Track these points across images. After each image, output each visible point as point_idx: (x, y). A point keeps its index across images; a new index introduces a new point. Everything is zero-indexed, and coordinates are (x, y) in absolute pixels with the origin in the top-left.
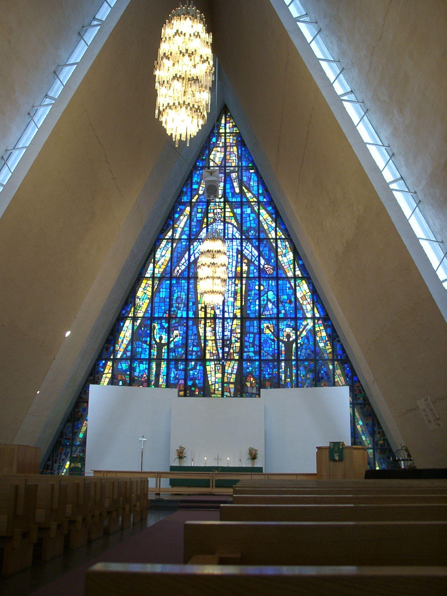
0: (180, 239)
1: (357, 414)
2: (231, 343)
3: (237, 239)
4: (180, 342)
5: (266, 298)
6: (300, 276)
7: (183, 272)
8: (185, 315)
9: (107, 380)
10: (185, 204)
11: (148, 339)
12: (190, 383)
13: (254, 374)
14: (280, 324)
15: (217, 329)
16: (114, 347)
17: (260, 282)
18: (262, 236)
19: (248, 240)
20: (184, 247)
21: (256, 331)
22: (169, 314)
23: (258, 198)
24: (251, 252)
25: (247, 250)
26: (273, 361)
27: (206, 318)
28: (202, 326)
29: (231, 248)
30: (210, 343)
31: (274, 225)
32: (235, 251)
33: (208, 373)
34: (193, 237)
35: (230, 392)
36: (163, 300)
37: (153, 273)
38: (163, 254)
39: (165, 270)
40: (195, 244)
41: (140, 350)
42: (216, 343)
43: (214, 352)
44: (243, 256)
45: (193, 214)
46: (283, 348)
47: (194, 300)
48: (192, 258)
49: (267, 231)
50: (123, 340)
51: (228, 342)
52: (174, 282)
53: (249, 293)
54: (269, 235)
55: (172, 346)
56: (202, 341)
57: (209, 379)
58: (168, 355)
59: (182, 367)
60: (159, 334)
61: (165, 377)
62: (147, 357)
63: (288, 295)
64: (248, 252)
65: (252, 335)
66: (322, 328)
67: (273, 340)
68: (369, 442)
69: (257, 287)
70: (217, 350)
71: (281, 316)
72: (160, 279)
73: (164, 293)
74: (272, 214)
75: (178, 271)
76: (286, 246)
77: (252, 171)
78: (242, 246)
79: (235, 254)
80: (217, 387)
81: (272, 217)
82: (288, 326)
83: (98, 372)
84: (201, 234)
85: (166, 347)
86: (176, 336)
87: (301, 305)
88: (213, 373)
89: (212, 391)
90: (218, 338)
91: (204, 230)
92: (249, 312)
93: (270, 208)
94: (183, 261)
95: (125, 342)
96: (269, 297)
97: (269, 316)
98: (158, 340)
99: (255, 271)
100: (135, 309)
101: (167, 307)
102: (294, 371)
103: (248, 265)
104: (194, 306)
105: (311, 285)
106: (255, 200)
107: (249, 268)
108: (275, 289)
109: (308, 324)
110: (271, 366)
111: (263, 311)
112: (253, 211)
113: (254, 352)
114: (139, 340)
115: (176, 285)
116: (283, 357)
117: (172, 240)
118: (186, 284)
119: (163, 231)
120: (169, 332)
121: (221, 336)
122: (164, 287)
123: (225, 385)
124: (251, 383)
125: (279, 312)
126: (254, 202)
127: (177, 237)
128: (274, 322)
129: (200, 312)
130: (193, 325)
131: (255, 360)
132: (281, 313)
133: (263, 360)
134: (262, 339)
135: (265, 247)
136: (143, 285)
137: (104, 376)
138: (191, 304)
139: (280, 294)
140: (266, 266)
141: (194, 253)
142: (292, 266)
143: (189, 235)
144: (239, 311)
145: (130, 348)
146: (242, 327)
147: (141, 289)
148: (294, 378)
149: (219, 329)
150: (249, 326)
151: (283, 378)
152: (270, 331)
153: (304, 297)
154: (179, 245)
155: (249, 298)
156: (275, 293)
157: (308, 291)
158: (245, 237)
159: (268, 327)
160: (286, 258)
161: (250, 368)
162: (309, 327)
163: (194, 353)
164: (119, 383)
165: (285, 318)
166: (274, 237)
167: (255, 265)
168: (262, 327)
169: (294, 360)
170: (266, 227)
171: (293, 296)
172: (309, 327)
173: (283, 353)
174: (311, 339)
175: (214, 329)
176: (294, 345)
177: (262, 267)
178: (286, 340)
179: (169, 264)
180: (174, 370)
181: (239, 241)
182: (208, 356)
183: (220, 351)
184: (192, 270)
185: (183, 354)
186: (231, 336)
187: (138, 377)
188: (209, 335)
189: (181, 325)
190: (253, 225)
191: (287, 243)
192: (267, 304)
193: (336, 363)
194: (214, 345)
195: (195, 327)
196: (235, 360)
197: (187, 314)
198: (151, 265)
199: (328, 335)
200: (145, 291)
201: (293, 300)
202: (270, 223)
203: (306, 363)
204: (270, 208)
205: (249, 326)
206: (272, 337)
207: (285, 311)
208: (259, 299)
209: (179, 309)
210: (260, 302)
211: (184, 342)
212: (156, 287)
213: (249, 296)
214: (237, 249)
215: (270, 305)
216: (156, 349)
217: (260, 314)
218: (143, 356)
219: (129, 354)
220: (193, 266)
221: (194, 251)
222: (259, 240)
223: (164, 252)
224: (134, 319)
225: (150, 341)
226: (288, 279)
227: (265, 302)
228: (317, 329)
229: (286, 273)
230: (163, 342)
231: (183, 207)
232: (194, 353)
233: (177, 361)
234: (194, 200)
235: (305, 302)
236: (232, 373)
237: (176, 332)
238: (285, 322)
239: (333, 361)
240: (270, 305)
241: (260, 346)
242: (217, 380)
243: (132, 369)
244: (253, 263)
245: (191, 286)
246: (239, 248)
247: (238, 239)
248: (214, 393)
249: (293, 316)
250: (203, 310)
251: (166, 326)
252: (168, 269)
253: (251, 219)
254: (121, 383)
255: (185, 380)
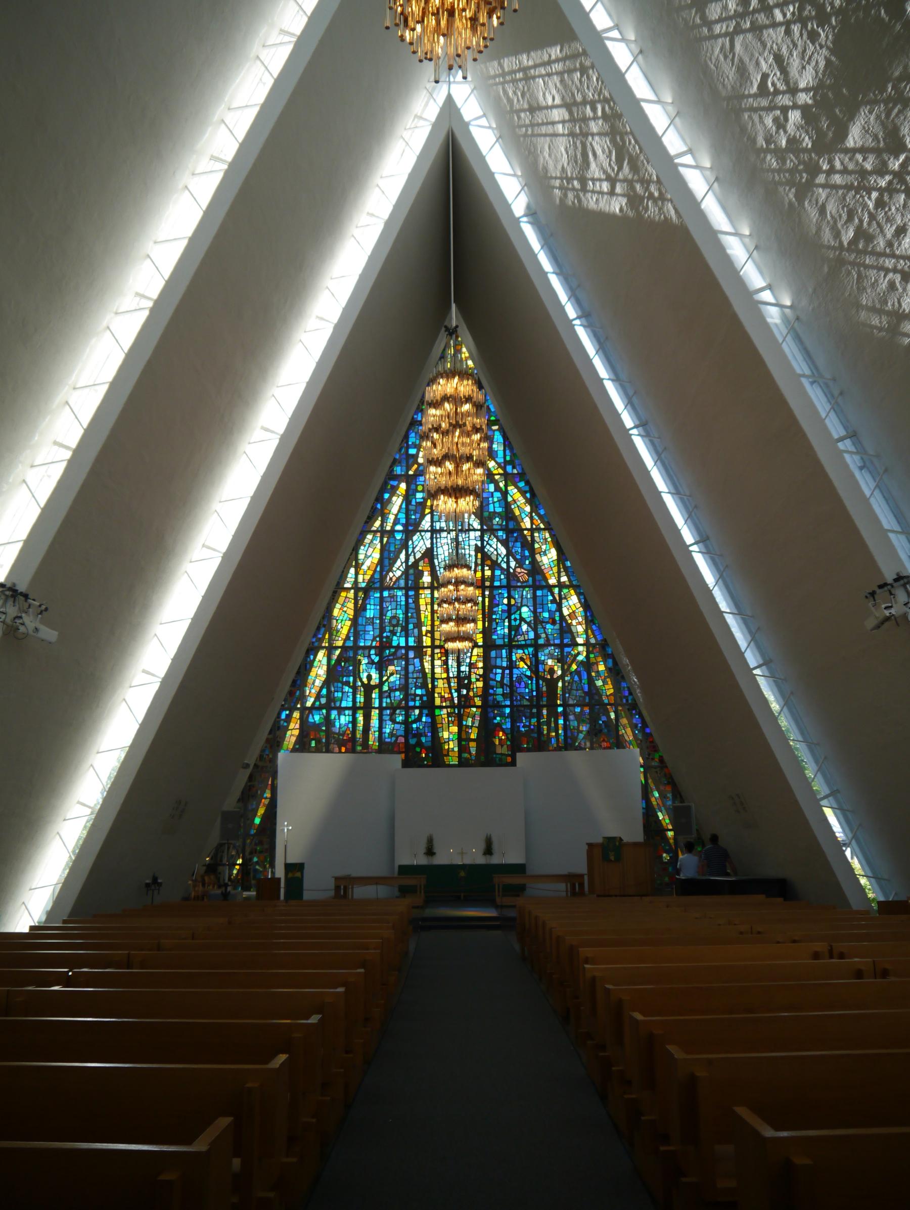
0: (393, 531)
1: (650, 781)
2: (470, 682)
3: (475, 530)
4: (398, 682)
5: (518, 617)
6: (568, 583)
7: (398, 579)
8: (403, 644)
9: (293, 739)
10: (398, 478)
11: (351, 679)
12: (413, 741)
13: (504, 727)
14: (539, 654)
15: (450, 662)
16: (304, 692)
17: (509, 593)
18: (511, 525)
19: (493, 531)
20: (398, 543)
21: (505, 664)
22: (381, 641)
23: (504, 469)
24: (496, 550)
25: (491, 546)
26: (531, 707)
27: (433, 647)
28: (428, 658)
29: (467, 543)
30: (440, 684)
31: (528, 509)
32: (472, 548)
33: (439, 726)
34: (411, 528)
35: (470, 753)
36: (371, 621)
37: (356, 582)
38: (369, 554)
39: (372, 576)
40: (415, 538)
41: (340, 694)
42: (449, 683)
43: (446, 696)
44: (485, 557)
45: (411, 492)
46: (544, 689)
47: (415, 621)
48: (412, 560)
49: (519, 519)
50: (314, 681)
51: (466, 682)
52: (386, 594)
53: (495, 609)
54: (522, 524)
55: (385, 688)
56: (429, 681)
57: (440, 735)
58: (381, 702)
59: (401, 718)
60: (368, 673)
61: (377, 734)
62: (350, 704)
63: (549, 611)
64: (492, 550)
65: (499, 671)
66: (600, 659)
67: (530, 678)
68: (667, 821)
69: (505, 601)
70: (451, 693)
71: (541, 641)
72: (367, 591)
73: (372, 611)
74: (526, 492)
75: (391, 579)
76: (546, 539)
77: (496, 427)
78: (482, 540)
79: (473, 553)
80: (451, 746)
81: (525, 497)
82: (551, 656)
83: (279, 728)
84: (423, 523)
85: (377, 690)
86: (392, 674)
87: (569, 625)
88: (445, 726)
89: (445, 753)
90: (451, 675)
91: (428, 518)
92: (494, 637)
93: (522, 484)
94: (398, 563)
95: (318, 683)
96: (524, 616)
97: (523, 643)
98: (365, 680)
99: (502, 577)
100: (331, 635)
101: (377, 632)
102: (561, 722)
103: (492, 569)
104: (416, 631)
105: (582, 597)
106: (501, 471)
107: (493, 573)
108: (531, 603)
109: (579, 653)
110: (528, 714)
111: (515, 635)
112: (497, 488)
113: (503, 695)
114: (338, 681)
115: (389, 599)
116: (544, 701)
117: (382, 532)
118: (403, 599)
119: (370, 519)
120: (381, 667)
121: (456, 673)
122: (372, 602)
123: (463, 743)
124: (500, 740)
125: (537, 636)
126: (499, 474)
127: (388, 528)
128: (531, 650)
129: (424, 638)
130: (414, 658)
131: (506, 706)
132: (540, 637)
133: (517, 706)
134: (515, 676)
135: (516, 541)
136: (341, 600)
137: (289, 733)
138: (411, 626)
139: (539, 610)
140: (518, 570)
141: (413, 551)
142: (555, 569)
143: (405, 526)
144: (481, 635)
145: (324, 691)
146: (486, 658)
147: (338, 606)
148: (560, 732)
149: (452, 662)
150: (496, 658)
151: (545, 732)
152: (526, 664)
153: (573, 615)
154: (392, 540)
155: (494, 617)
156: (532, 608)
157: (579, 605)
158: (487, 529)
159: (522, 659)
160: (548, 557)
161: (498, 718)
162: (580, 658)
163: (418, 698)
164: (310, 744)
165: (548, 644)
166: (529, 526)
167: (502, 569)
168: (514, 659)
169: (560, 705)
170: (517, 513)
171: (557, 614)
172: (580, 658)
173: (545, 695)
174: (585, 676)
175: (446, 663)
176: (560, 684)
177: (511, 571)
178: (549, 677)
179: (378, 569)
180: (389, 723)
181: (478, 533)
182: (438, 702)
183: (455, 695)
184: (412, 577)
185: (401, 700)
186: (470, 672)
187: (339, 734)
188: (438, 670)
189: (397, 659)
190: (499, 510)
191: (547, 535)
192: (520, 625)
193: (620, 708)
194: (446, 685)
195: (417, 661)
196: (477, 707)
197: (407, 641)
198: (352, 570)
199: (609, 669)
200: (345, 609)
201: (557, 618)
202: (523, 506)
203: (578, 710)
204: (522, 484)
205: (496, 658)
206: (528, 673)
207: (547, 635)
208: (509, 618)
209: (394, 633)
210: (510, 622)
211: (403, 681)
212: (360, 602)
213: (495, 613)
214: (476, 545)
215: (524, 627)
216: (362, 693)
217: (511, 640)
218: (344, 704)
219: (323, 701)
220: (411, 571)
221: (414, 548)
222: (509, 532)
223: (371, 550)
224: (331, 649)
225: (355, 681)
226: (550, 588)
227: (518, 622)
228: (593, 660)
229: (546, 580)
230: (372, 683)
231: (395, 483)
232: (418, 698)
233: (393, 709)
234: (411, 473)
235: (574, 622)
236: (472, 726)
237: (391, 668)
238: (547, 651)
239: (615, 705)
240: (524, 627)
241: (511, 685)
242: (451, 736)
243: (328, 721)
244: (499, 565)
245: (410, 601)
246: (479, 544)
247: (478, 530)
248: (448, 755)
249: (557, 642)
250: (429, 635)
251: (376, 659)
252: (377, 576)
253: (496, 500)
254: (313, 744)
255: (406, 736)
